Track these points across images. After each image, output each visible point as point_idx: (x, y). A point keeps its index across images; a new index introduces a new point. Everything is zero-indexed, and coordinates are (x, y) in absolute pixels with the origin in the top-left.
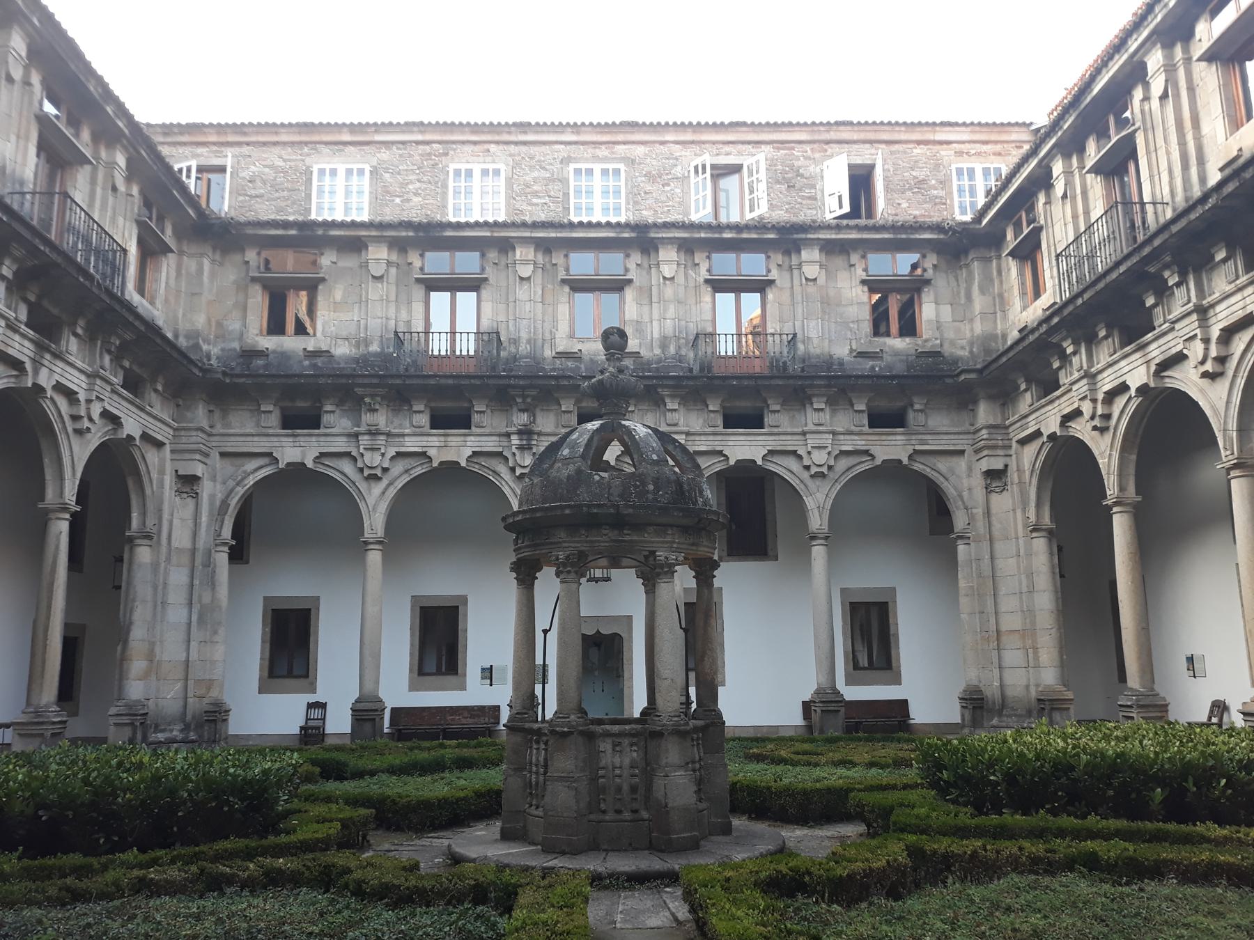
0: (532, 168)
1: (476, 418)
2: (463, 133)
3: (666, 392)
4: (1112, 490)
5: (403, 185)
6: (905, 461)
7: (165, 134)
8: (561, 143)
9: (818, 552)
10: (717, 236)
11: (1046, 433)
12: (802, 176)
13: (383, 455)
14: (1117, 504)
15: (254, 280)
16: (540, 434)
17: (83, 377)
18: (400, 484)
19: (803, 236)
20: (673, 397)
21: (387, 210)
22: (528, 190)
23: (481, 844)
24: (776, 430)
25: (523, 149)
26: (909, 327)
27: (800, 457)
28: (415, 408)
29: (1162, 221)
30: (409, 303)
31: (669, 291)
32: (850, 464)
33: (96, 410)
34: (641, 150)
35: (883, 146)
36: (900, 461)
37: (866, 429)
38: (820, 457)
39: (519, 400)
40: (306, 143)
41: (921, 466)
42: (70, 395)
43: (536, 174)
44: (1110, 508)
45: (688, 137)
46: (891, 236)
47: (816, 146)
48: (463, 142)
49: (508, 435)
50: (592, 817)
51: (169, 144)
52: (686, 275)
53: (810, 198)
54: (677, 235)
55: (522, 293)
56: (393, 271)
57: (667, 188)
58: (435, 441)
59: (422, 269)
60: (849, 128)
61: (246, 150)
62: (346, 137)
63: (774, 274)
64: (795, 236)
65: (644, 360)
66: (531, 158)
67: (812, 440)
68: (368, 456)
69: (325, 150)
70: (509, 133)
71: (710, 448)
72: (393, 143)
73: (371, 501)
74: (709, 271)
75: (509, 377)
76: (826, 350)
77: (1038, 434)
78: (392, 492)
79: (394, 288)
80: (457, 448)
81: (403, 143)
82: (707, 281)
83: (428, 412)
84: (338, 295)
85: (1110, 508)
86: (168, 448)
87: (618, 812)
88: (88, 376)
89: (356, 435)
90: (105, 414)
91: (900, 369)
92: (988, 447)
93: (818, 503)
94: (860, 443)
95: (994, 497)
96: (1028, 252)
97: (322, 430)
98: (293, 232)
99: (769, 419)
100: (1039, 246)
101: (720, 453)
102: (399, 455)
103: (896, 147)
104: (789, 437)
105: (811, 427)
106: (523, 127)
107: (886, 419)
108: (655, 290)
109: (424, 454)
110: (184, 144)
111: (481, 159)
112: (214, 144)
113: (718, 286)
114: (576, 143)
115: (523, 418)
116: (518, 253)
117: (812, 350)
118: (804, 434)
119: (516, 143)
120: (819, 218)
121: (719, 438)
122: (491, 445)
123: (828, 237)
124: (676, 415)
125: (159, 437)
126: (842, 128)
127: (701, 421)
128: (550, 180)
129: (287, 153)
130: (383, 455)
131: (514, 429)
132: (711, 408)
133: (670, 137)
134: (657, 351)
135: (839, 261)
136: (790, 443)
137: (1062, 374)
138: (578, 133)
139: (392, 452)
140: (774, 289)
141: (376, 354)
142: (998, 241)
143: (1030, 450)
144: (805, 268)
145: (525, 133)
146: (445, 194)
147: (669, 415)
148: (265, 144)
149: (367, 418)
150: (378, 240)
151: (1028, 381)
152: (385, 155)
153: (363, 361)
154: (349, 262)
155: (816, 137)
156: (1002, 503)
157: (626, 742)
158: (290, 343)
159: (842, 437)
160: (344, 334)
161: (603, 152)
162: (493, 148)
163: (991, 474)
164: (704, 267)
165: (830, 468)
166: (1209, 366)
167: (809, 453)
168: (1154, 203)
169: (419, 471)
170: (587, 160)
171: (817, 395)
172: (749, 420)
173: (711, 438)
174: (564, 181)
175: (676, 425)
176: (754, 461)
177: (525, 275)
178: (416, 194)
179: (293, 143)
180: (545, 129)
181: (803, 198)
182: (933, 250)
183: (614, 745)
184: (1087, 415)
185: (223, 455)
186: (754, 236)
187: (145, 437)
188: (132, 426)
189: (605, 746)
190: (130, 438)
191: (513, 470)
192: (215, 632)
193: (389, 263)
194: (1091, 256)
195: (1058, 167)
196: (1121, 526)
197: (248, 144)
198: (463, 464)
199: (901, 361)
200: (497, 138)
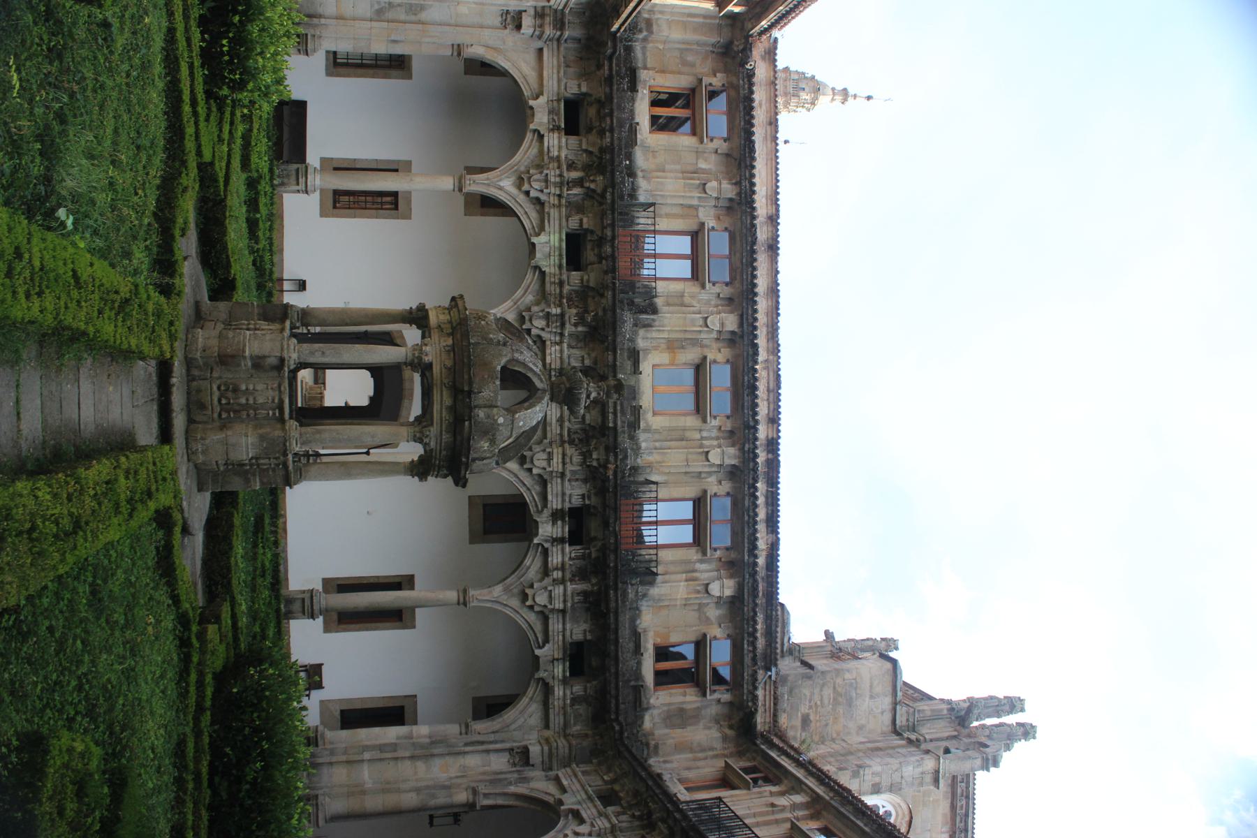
11: (564, 797)
15: (701, 80)
23: (190, 272)
26: (663, 678)
30: (682, 216)
77: (563, 790)
92: (550, 750)
100: (733, 788)
113: (699, 504)
142: (740, 754)
151: (614, 781)
156: (499, 763)
158: (642, 112)
163: (525, 752)
165: (531, 607)
185: (541, 50)
195: (798, 799)
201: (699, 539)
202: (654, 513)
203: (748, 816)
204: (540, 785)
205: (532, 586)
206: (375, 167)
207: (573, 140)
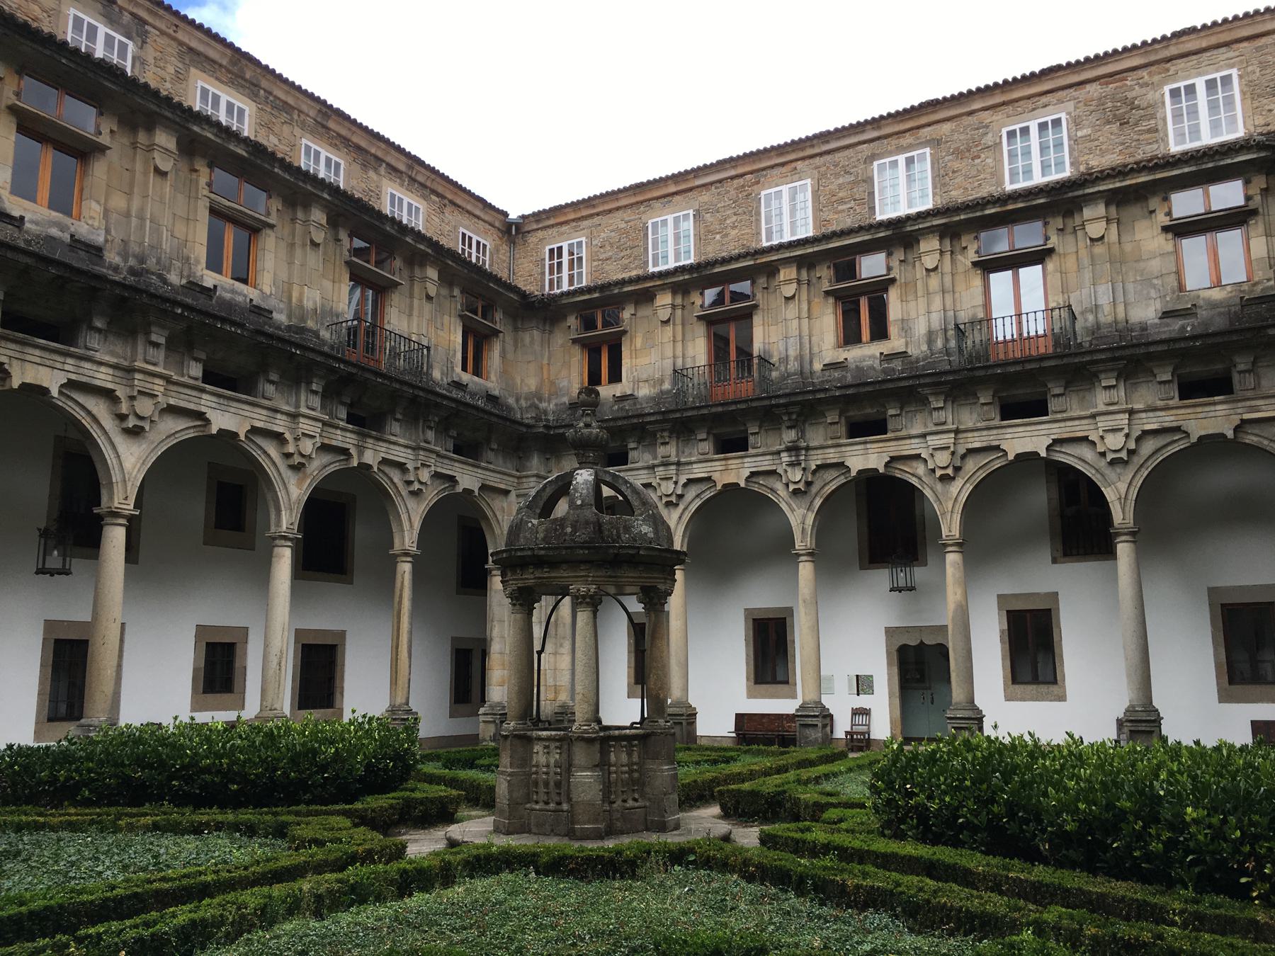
0: (837, 175)
1: (751, 439)
2: (770, 158)
3: (927, 391)
5: (722, 221)
6: (1230, 434)
7: (538, 221)
8: (864, 142)
10: (978, 214)
12: (1138, 108)
13: (676, 483)
15: (574, 341)
16: (807, 449)
17: (409, 451)
18: (693, 507)
19: (1080, 192)
20: (935, 394)
21: (710, 249)
22: (834, 198)
24: (1059, 416)
25: (828, 158)
27: (1093, 443)
28: (699, 437)
31: (934, 282)
32: (1165, 442)
33: (425, 475)
34: (947, 127)
35: (1245, 44)
36: (1223, 435)
37: (1176, 401)
38: (1115, 441)
39: (785, 418)
40: (642, 202)
41: (1256, 439)
42: (401, 467)
43: (841, 180)
45: (998, 99)
46: (1193, 169)
47: (1153, 68)
48: (772, 167)
49: (779, 453)
50: (528, 806)
51: (541, 229)
52: (953, 261)
53: (1149, 131)
54: (935, 223)
55: (791, 311)
56: (679, 312)
57: (977, 161)
58: (718, 465)
59: (702, 306)
60: (1192, 36)
61: (596, 220)
62: (672, 189)
63: (1054, 241)
64: (1070, 195)
65: (913, 359)
66: (836, 166)
67: (1103, 423)
68: (664, 484)
69: (657, 204)
70: (812, 146)
71: (984, 444)
72: (712, 184)
73: (672, 524)
74: (977, 252)
75: (769, 398)
76: (1121, 315)
78: (687, 516)
79: (679, 328)
80: (735, 471)
81: (720, 181)
82: (975, 264)
83: (711, 438)
84: (639, 342)
86: (513, 494)
87: (547, 803)
88: (413, 449)
89: (653, 467)
90: (437, 476)
91: (1220, 324)
94: (1168, 419)
97: (629, 466)
98: (596, 295)
99: (1053, 405)
101: (997, 448)
102: (690, 482)
103: (1263, 41)
104: (1077, 423)
105: (1102, 408)
106: (824, 136)
107: (1200, 386)
108: (919, 284)
109: (709, 479)
110: (553, 226)
111: (789, 179)
112: (573, 220)
114: (879, 138)
115: (790, 436)
116: (782, 273)
117: (1102, 319)
118: (1093, 416)
119: (821, 154)
120: (1161, 152)
121: (995, 432)
122: (765, 464)
123: (1111, 186)
124: (942, 413)
125: (503, 486)
126: (1184, 38)
127: (975, 416)
128: (855, 183)
129: (627, 215)
130: (676, 483)
131: (783, 447)
132: (982, 400)
133: (977, 105)
134: (925, 348)
135: (1135, 210)
136: (1078, 429)
138: (879, 128)
139: (683, 480)
140: (1055, 257)
141: (669, 392)
144: (1089, 228)
145: (828, 142)
146: (758, 221)
147: (935, 414)
148: (610, 211)
149: (662, 451)
150: (662, 288)
152: (705, 197)
154: (644, 311)
155: (1153, 58)
157: (553, 745)
159: (1143, 415)
160: (644, 377)
161: (908, 139)
162: (799, 165)
167: (1102, 438)
169: (708, 495)
170: (890, 154)
171: (1105, 371)
172: (1034, 408)
173: (985, 433)
174: (869, 181)
175: (944, 423)
176: (1037, 454)
177: (789, 294)
178: (734, 227)
179: (632, 205)
180: (845, 133)
181: (1141, 133)
182: (1259, 172)
183: (546, 747)
186: (1021, 205)
187: (484, 488)
188: (468, 479)
189: (538, 748)
190: (468, 492)
191: (787, 485)
192: (561, 645)
193: (674, 307)
197: (598, 214)
198: (743, 485)
199: (1220, 314)
200: (801, 154)
201: (1038, 257)
202: (1008, 320)
205: (1103, 454)
206: (591, 653)
207: (632, 455)
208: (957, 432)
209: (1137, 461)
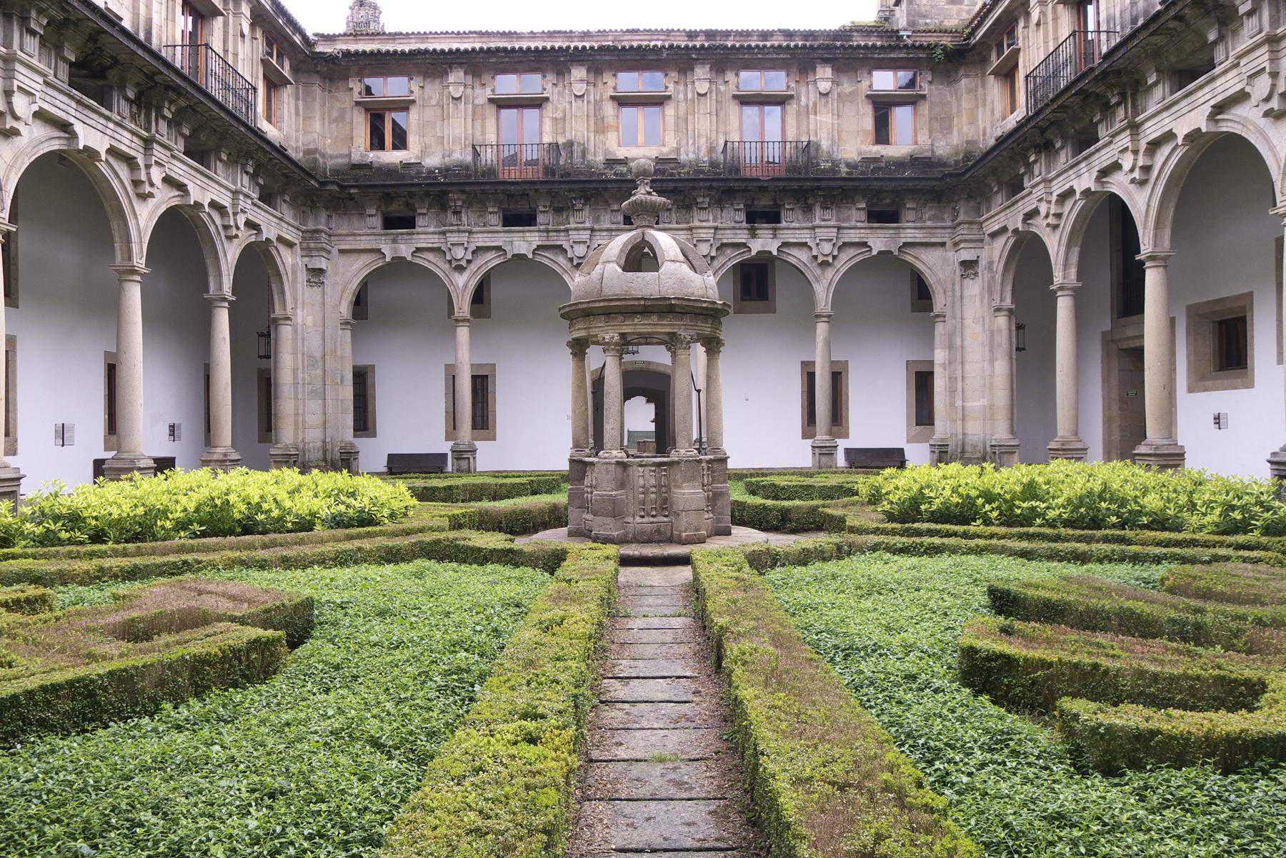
4: (1058, 278)
9: (822, 329)
11: (1011, 229)
14: (1061, 288)
15: (358, 103)
29: (1113, 44)
30: (483, 120)
33: (241, 220)
36: (891, 252)
44: (1055, 292)
77: (1004, 230)
85: (1055, 292)
93: (823, 290)
95: (967, 281)
96: (1007, 73)
100: (1016, 66)
107: (883, 215)
118: (813, 228)
137: (1026, 179)
142: (985, 60)
143: (1001, 240)
151: (1000, 184)
153: (446, 170)
156: (973, 288)
164: (732, 86)
165: (834, 257)
166: (1136, 174)
168: (1108, 32)
184: (1043, 213)
185: (341, 251)
194: (1056, 74)
196: (1064, 307)
201: (780, 101)
203: (1046, 48)
204: (996, 251)
205: (815, 257)
207: (420, 221)
208: (716, 228)
209: (838, 264)
